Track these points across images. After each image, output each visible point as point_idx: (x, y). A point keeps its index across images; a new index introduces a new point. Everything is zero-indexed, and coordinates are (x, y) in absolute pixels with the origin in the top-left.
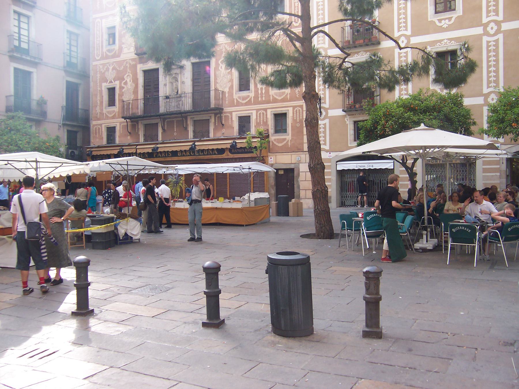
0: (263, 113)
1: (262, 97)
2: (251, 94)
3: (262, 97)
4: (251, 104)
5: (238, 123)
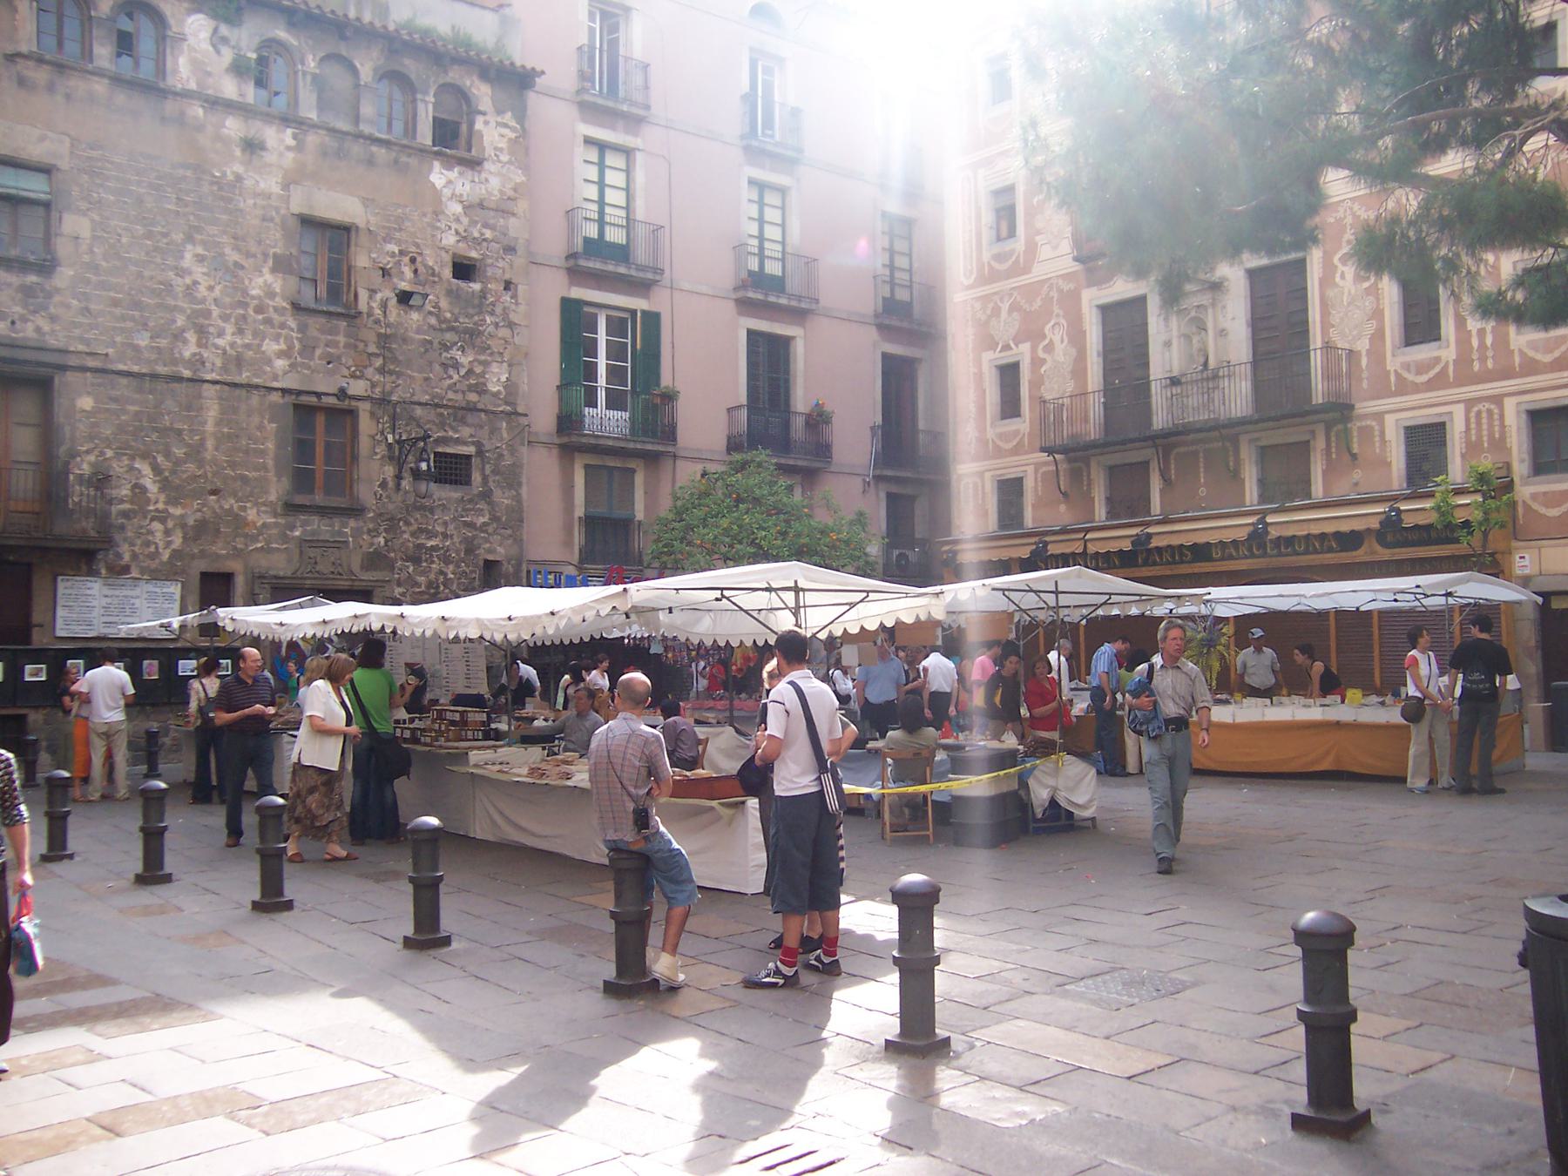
0: (1489, 412)
1: (1483, 359)
2: (1445, 351)
3: (1483, 359)
5: (1402, 448)
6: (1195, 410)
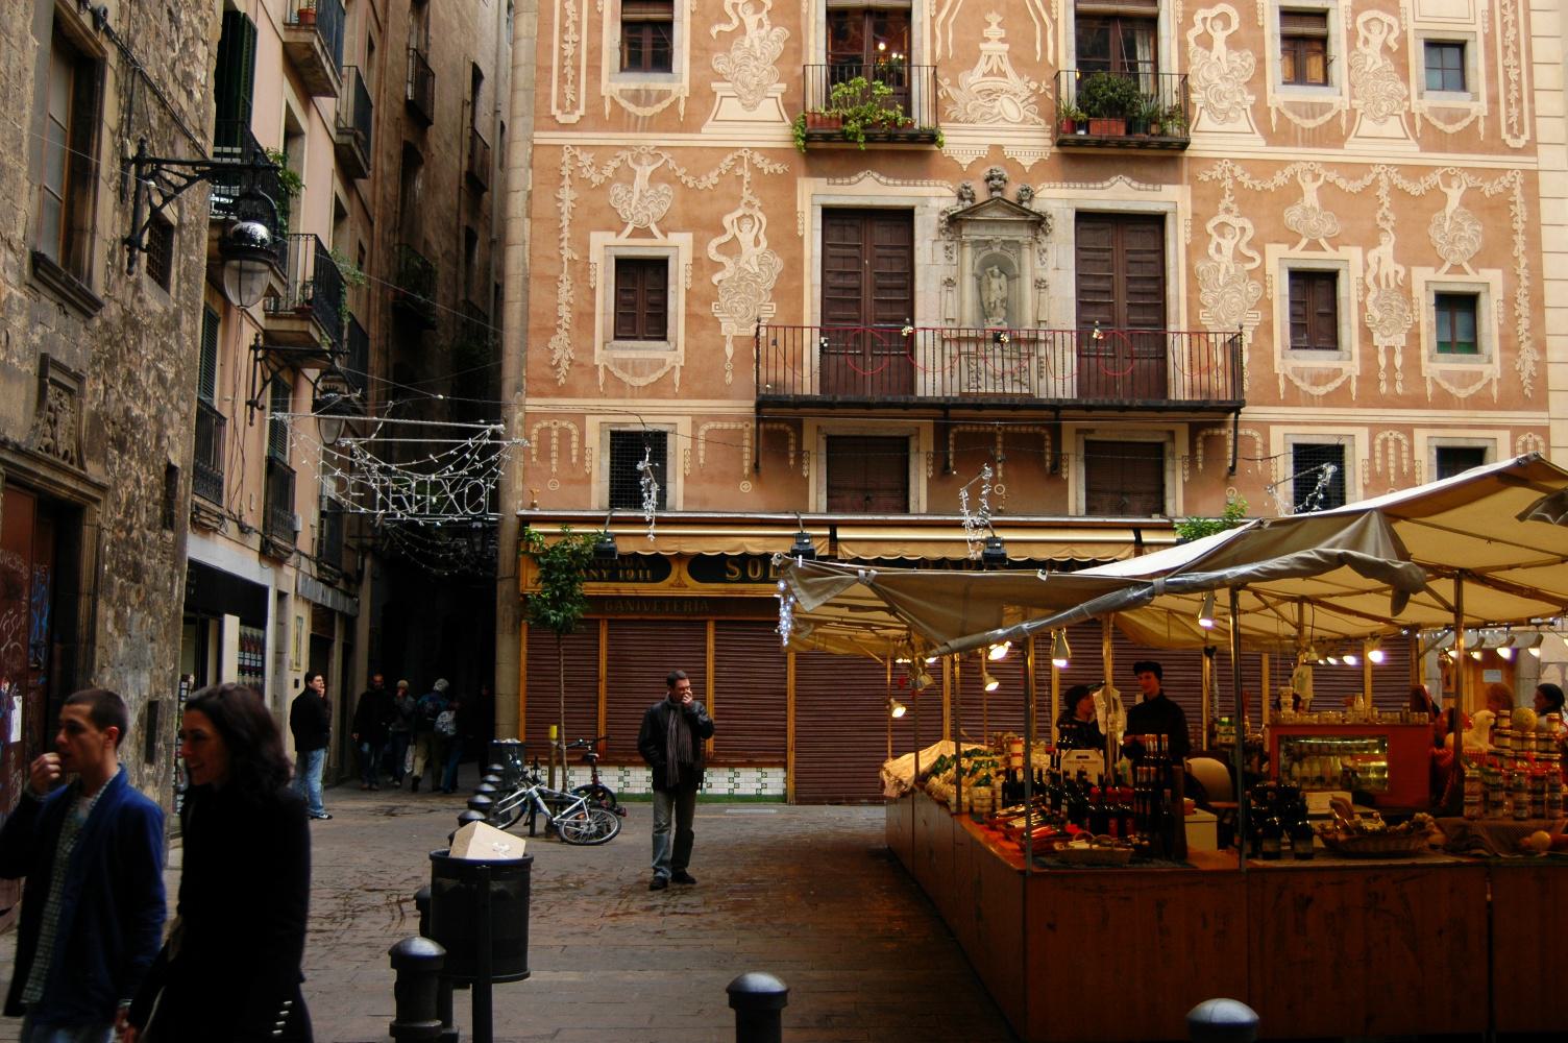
0: (1397, 441)
1: (1392, 382)
2: (1346, 362)
3: (1392, 382)
4: (1350, 404)
6: (993, 377)
